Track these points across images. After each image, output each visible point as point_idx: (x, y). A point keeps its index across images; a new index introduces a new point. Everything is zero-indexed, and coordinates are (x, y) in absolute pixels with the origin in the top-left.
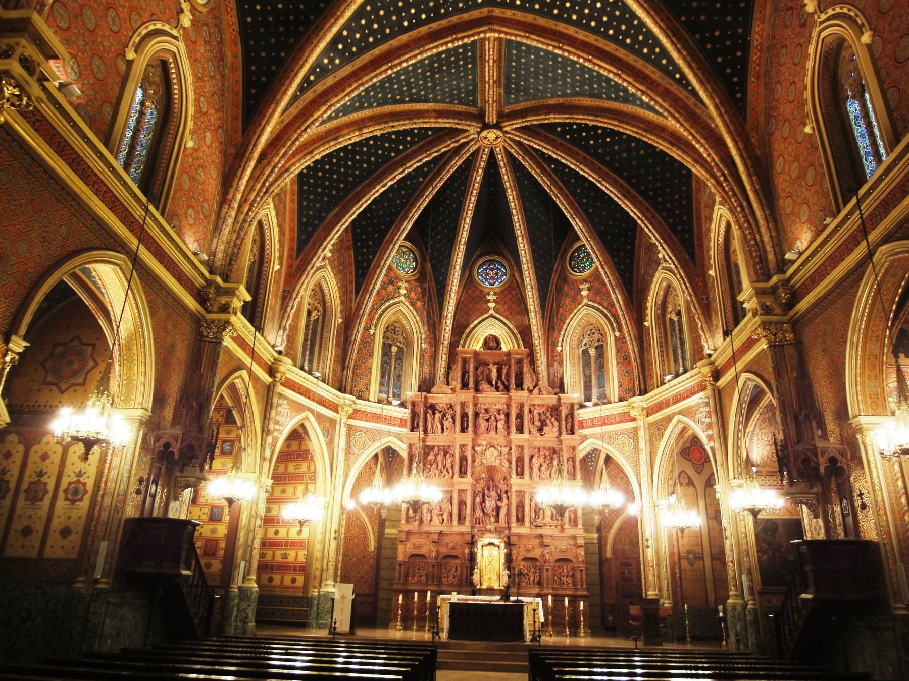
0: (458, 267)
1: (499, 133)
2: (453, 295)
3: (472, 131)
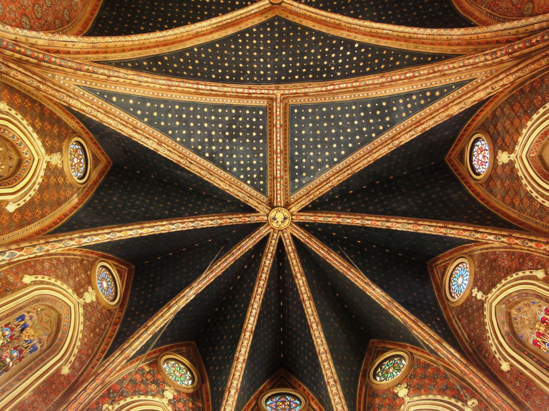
0: (241, 359)
1: (286, 214)
2: (233, 391)
3: (262, 213)
